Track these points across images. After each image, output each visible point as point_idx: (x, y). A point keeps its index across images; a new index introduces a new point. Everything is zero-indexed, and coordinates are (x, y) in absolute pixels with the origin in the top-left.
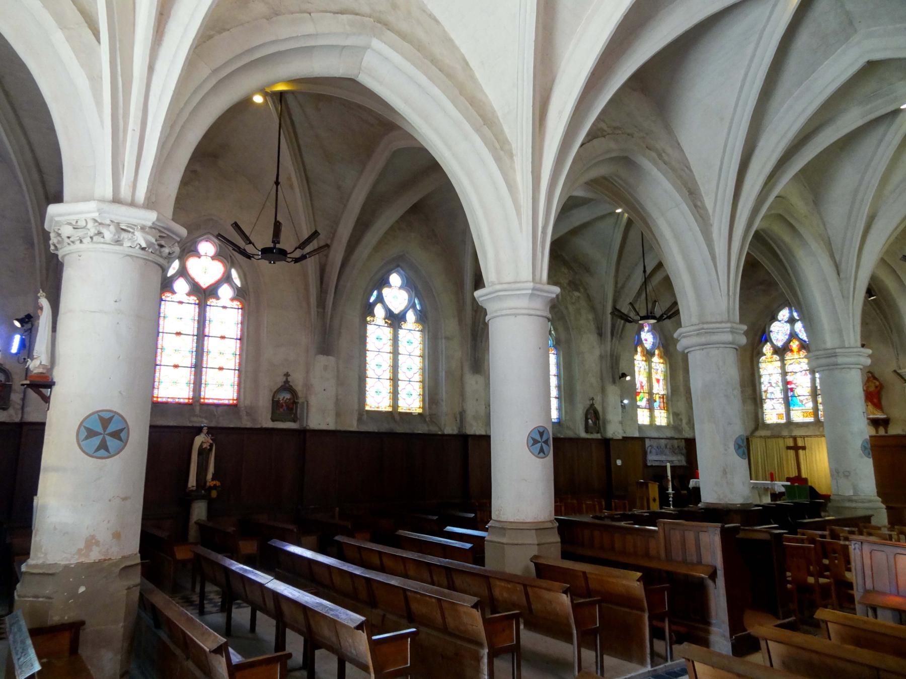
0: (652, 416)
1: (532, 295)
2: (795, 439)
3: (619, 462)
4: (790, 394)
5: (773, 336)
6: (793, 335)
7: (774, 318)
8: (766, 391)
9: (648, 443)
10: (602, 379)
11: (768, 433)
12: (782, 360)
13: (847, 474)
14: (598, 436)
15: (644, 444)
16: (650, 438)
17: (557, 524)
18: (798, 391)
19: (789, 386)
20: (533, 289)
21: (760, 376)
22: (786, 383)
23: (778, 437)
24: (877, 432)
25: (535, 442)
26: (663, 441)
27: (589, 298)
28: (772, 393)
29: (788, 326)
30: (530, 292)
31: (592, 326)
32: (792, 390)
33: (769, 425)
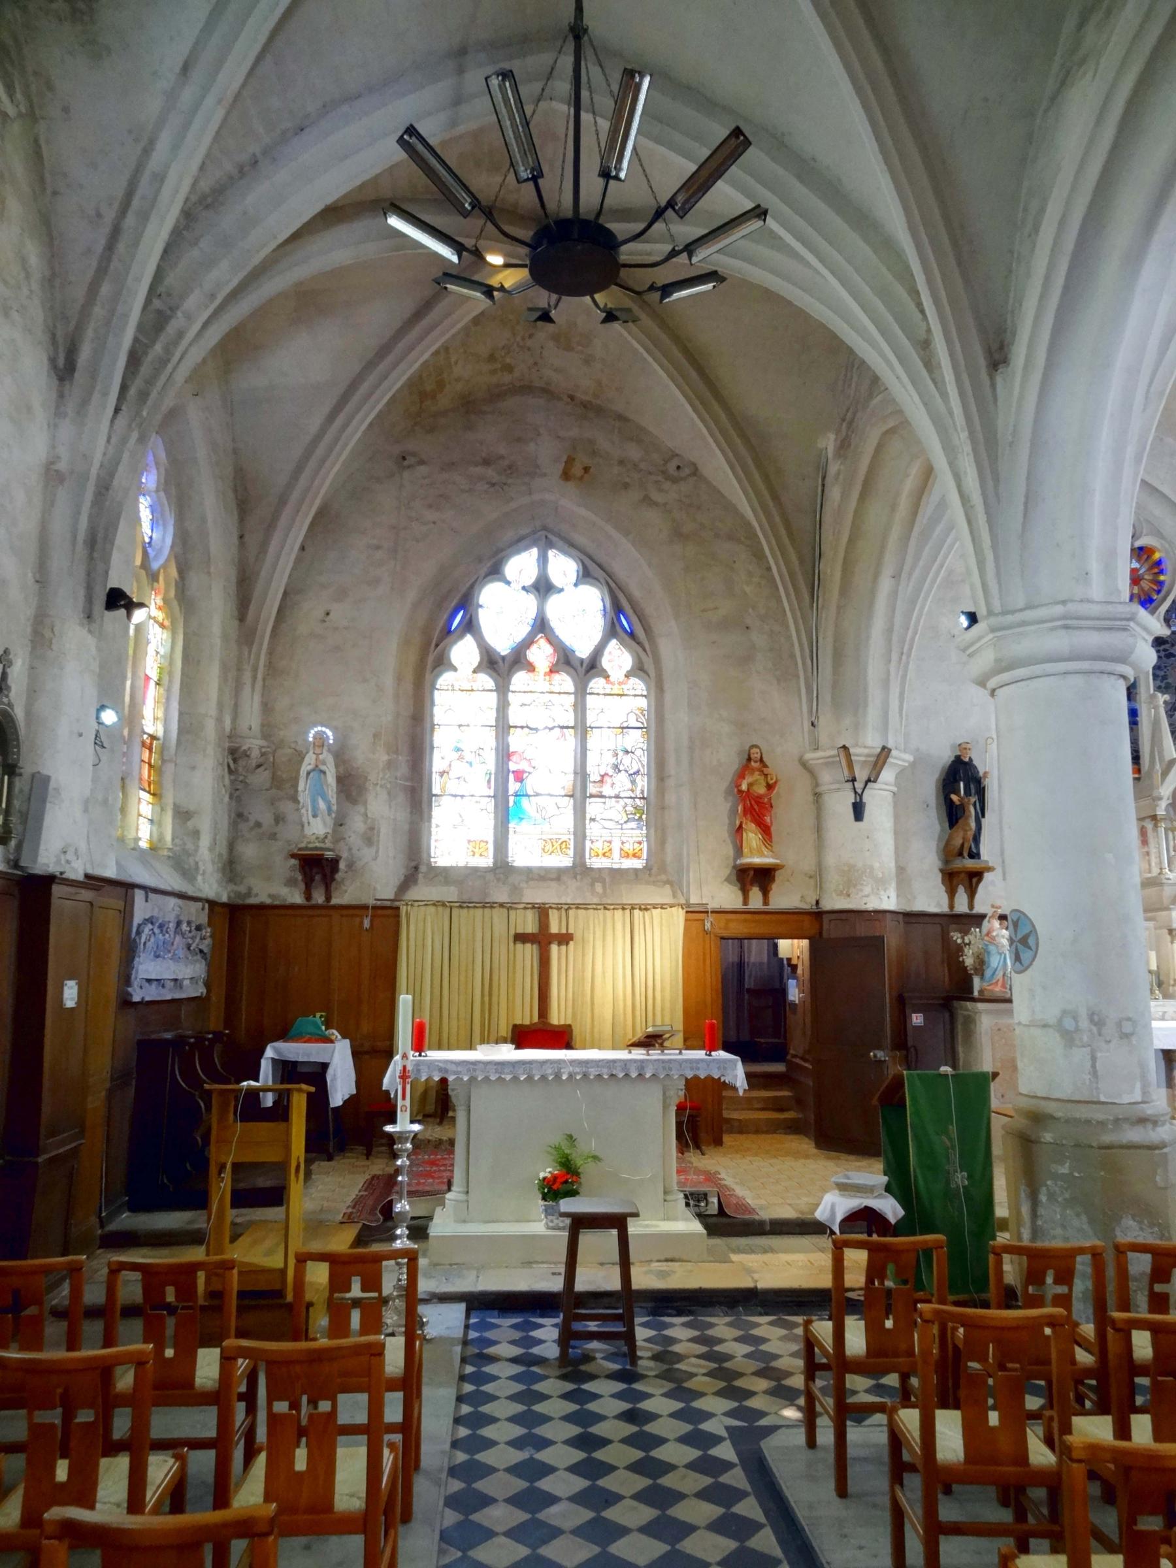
2: (543, 911)
3: (70, 994)
4: (513, 786)
5: (485, 618)
6: (541, 626)
7: (495, 572)
9: (142, 909)
10: (42, 580)
11: (450, 894)
12: (502, 689)
13: (1127, 1027)
15: (127, 913)
22: (504, 754)
24: (745, 902)
26: (172, 902)
29: (530, 602)
32: (519, 776)
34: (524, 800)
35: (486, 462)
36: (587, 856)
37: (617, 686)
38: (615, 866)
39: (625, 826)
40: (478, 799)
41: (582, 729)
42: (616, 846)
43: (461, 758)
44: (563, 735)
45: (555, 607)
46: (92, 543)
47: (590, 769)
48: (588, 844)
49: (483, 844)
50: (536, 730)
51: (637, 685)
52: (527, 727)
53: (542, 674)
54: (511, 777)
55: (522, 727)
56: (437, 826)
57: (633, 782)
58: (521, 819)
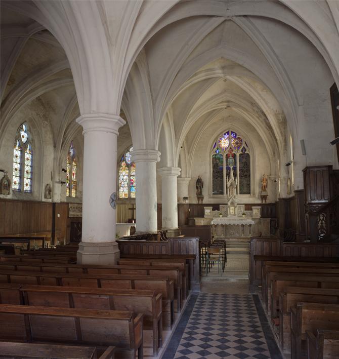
0: (70, 192)
1: (117, 122)
3: (59, 215)
8: (121, 183)
9: (70, 205)
12: (130, 170)
14: (50, 200)
16: (71, 203)
17: (117, 244)
20: (119, 120)
23: (125, 204)
25: (113, 200)
27: (52, 127)
28: (123, 184)
30: (117, 121)
31: (51, 141)
32: (132, 183)
33: (121, 199)
35: (125, 134)
43: (123, 181)
46: (59, 165)
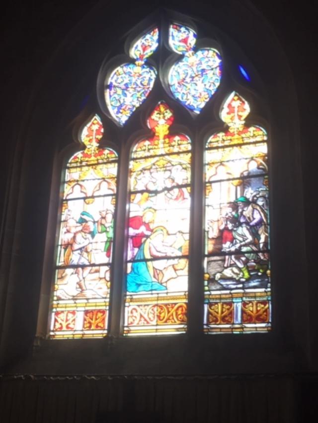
5: (111, 100)
6: (160, 95)
8: (68, 246)
18: (154, 244)
19: (132, 232)
21: (60, 203)
29: (149, 76)
32: (138, 241)
34: (141, 265)
36: (205, 321)
37: (236, 136)
38: (236, 332)
39: (246, 285)
40: (97, 268)
41: (198, 187)
42: (238, 306)
44: (182, 194)
45: (174, 75)
47: (207, 226)
48: (206, 307)
49: (100, 315)
50: (156, 192)
51: (259, 133)
52: (147, 191)
53: (161, 137)
54: (130, 245)
55: (142, 192)
56: (59, 299)
57: (256, 235)
58: (139, 285)
